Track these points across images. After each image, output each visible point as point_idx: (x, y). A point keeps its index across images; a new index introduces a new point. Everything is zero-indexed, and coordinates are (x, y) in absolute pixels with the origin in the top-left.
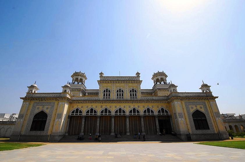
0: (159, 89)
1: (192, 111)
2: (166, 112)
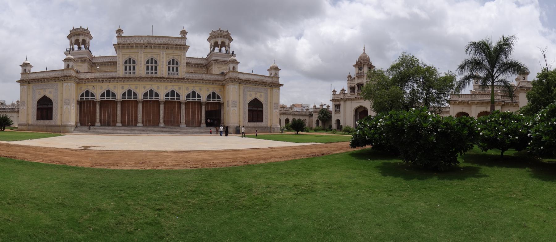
0: (216, 61)
1: (250, 99)
2: (218, 97)
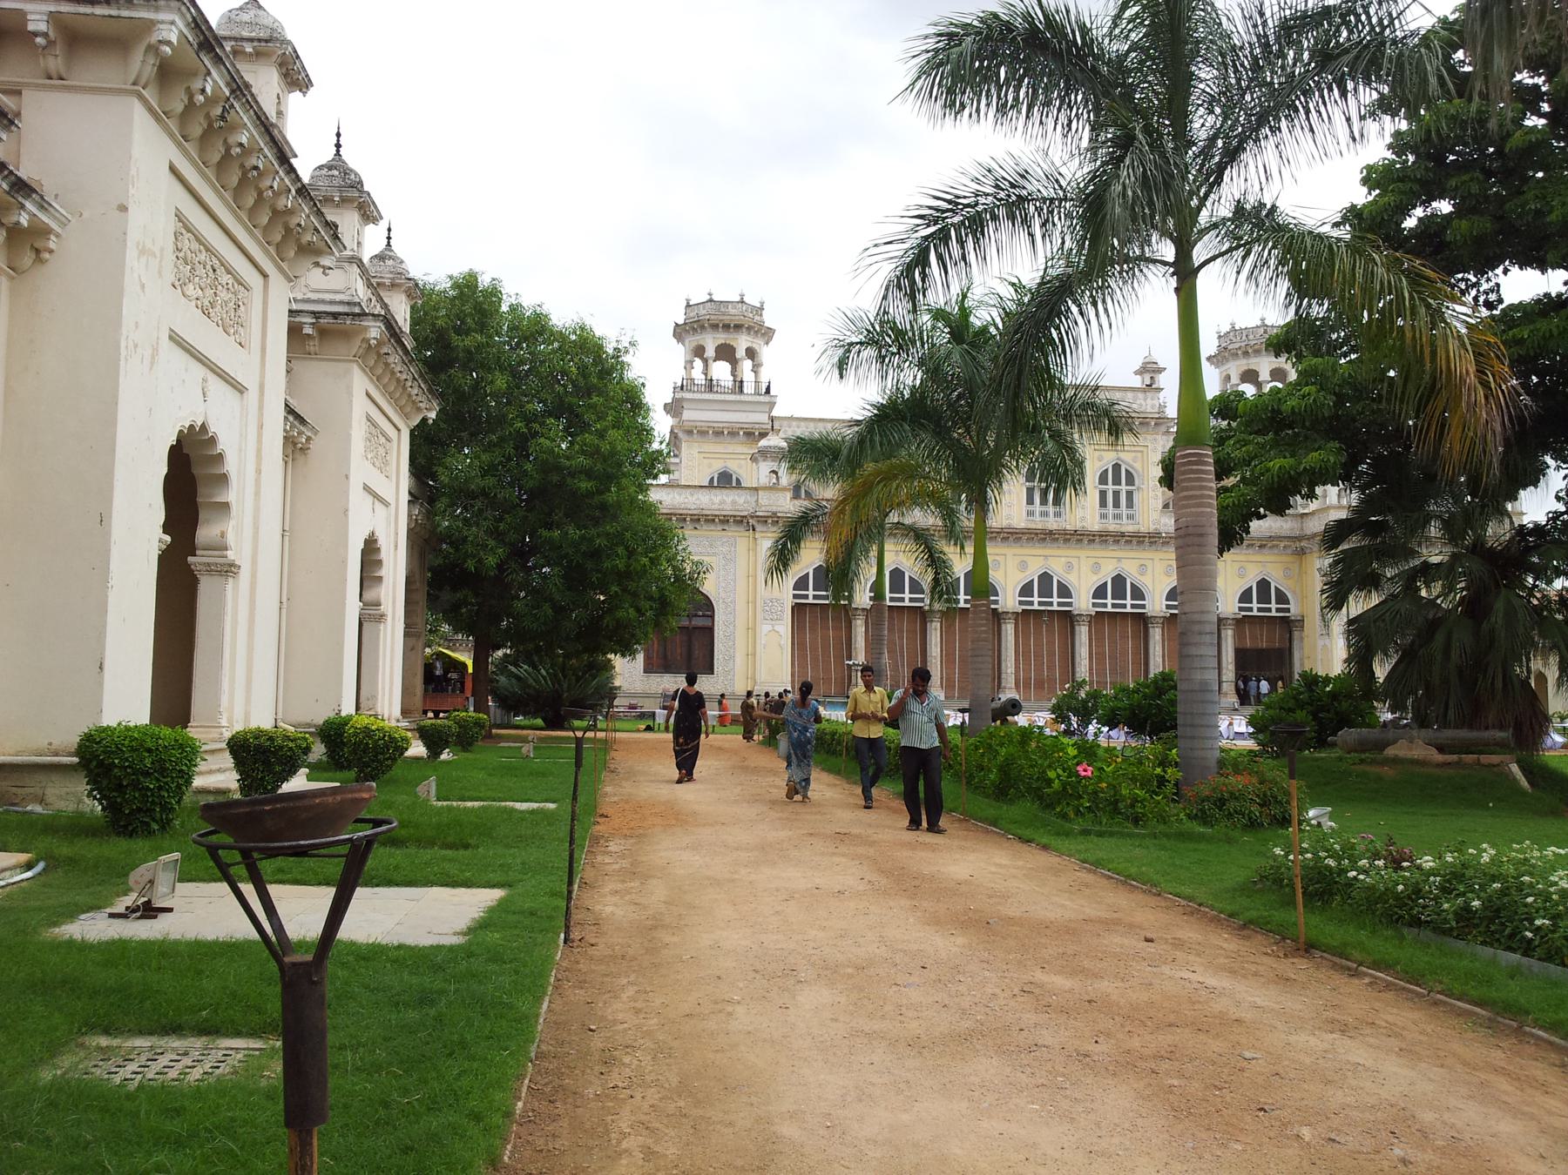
2: (1282, 598)
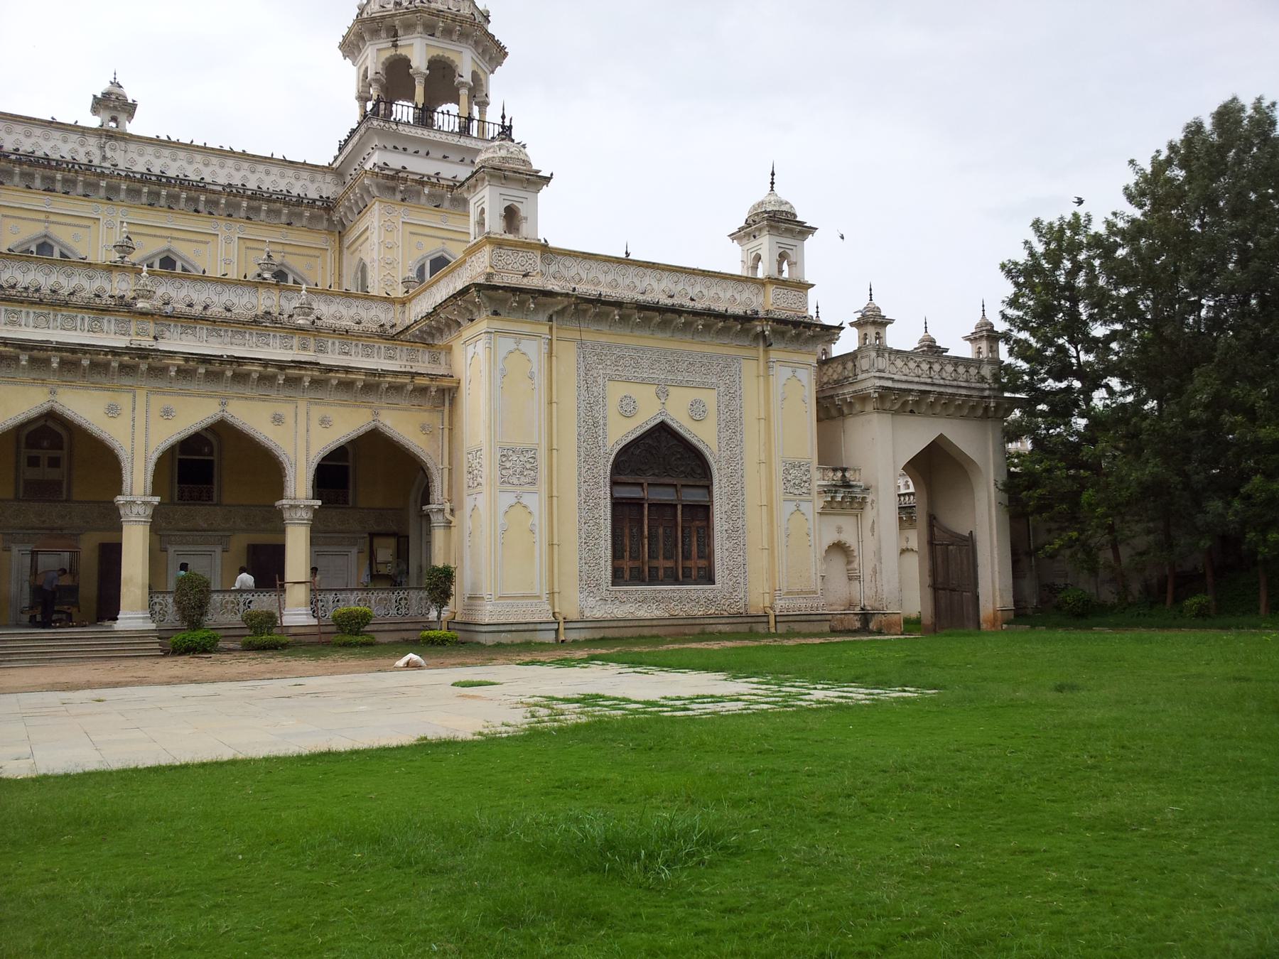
0: (394, 184)
